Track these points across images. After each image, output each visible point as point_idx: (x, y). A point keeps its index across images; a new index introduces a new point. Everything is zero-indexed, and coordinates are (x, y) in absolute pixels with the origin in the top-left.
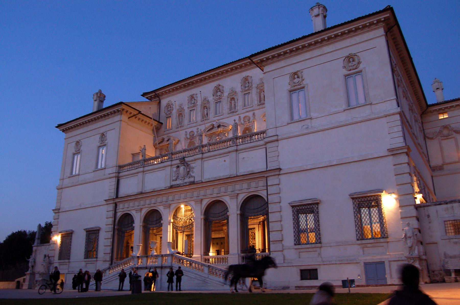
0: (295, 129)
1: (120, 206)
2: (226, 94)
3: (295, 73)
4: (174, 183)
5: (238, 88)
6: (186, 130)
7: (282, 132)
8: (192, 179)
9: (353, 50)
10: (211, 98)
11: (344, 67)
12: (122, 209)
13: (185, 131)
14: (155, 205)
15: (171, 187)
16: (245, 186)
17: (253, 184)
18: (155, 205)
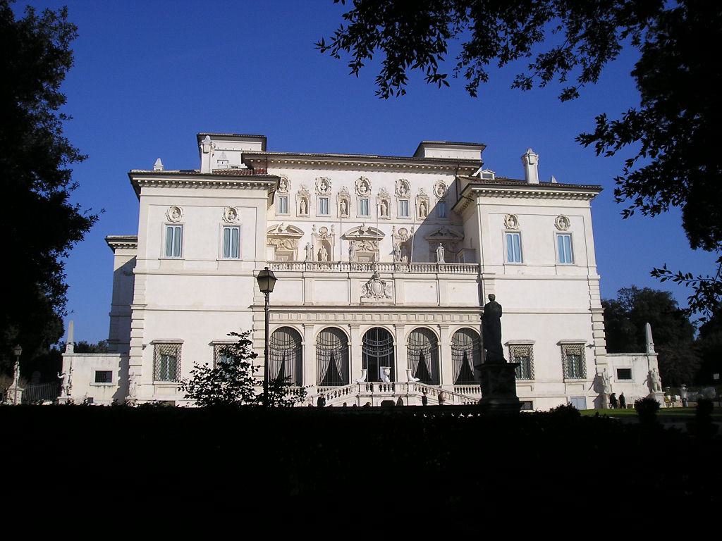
0: (512, 271)
1: (274, 317)
2: (374, 192)
3: (512, 216)
4: (363, 300)
5: (391, 191)
6: (315, 223)
7: (499, 272)
8: (390, 300)
9: (565, 212)
10: (352, 192)
11: (556, 226)
12: (277, 321)
13: (313, 223)
14: (337, 322)
15: (361, 306)
16: (456, 317)
17: (465, 317)
18: (337, 322)
